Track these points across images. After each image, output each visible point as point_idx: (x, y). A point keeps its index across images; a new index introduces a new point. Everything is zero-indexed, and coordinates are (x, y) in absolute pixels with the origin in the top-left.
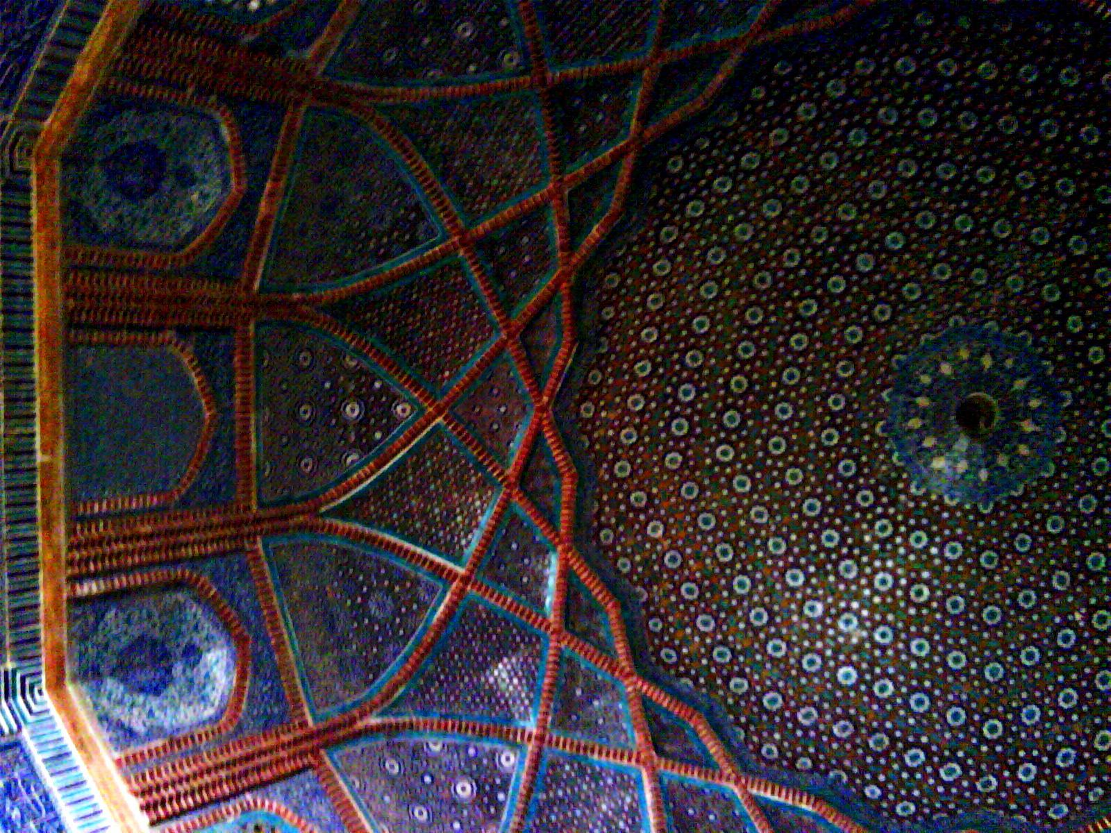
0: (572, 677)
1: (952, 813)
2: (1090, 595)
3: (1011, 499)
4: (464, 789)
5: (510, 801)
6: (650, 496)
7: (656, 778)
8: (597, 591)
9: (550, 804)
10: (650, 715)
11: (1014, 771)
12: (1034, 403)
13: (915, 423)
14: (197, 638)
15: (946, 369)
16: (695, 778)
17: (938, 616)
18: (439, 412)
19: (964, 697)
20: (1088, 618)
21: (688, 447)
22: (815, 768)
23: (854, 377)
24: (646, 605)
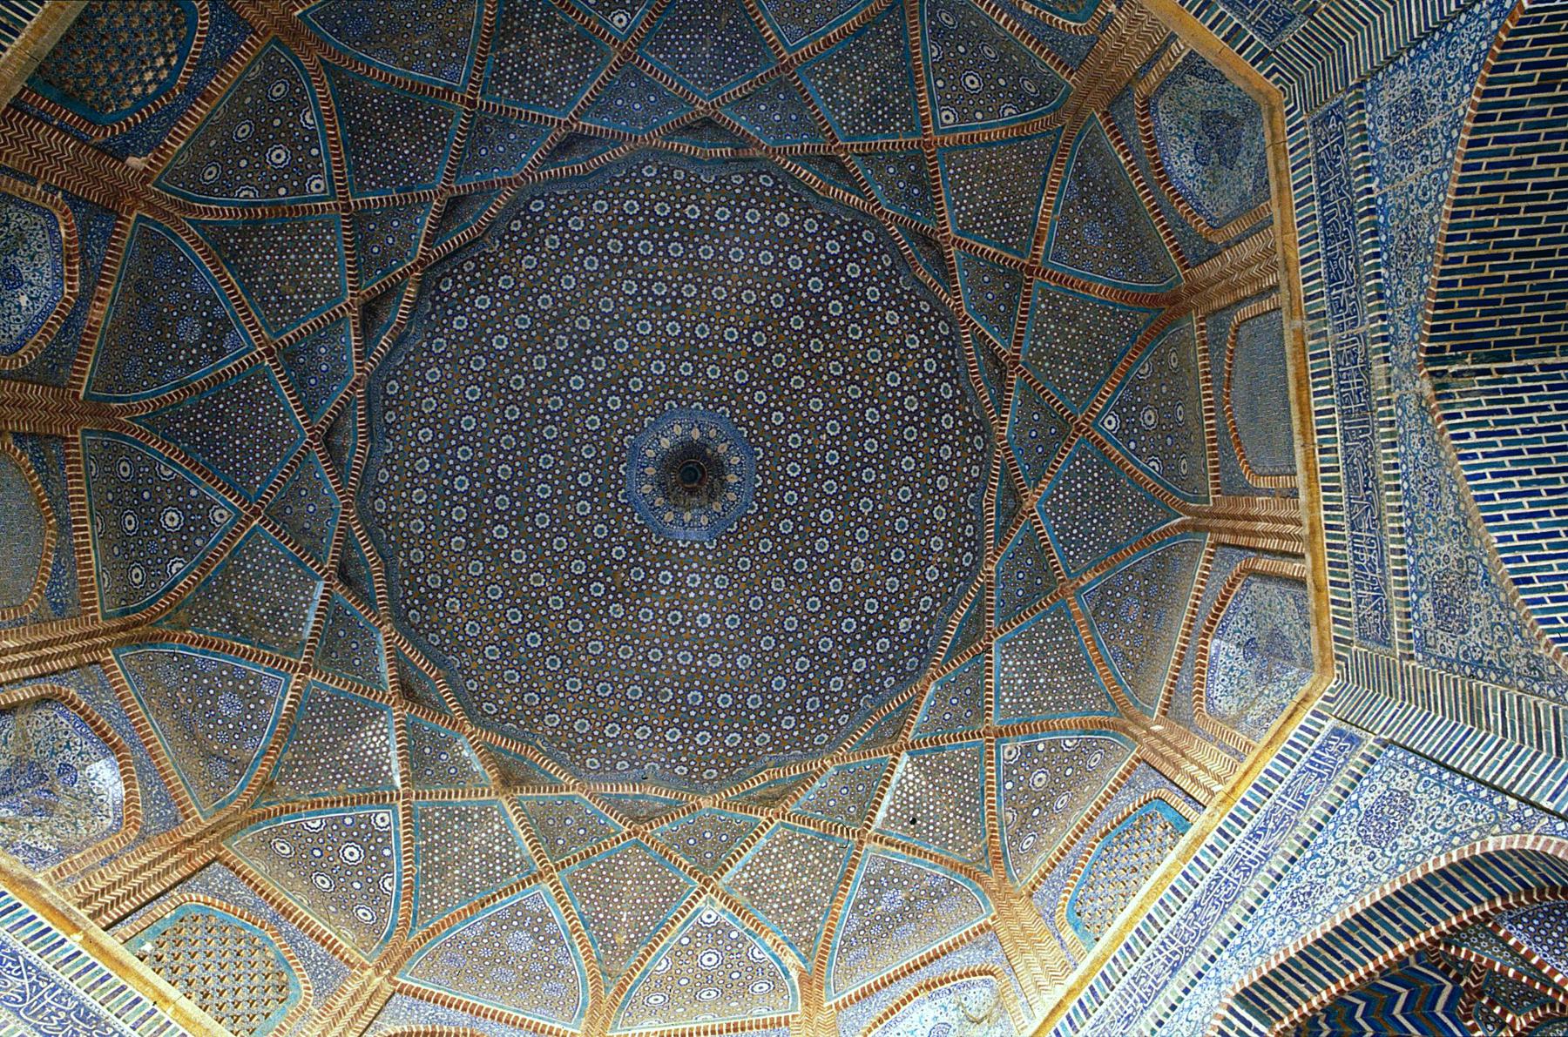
2: (801, 590)
6: (443, 576)
10: (490, 754)
11: (778, 725)
14: (69, 756)
18: (256, 513)
22: (632, 766)
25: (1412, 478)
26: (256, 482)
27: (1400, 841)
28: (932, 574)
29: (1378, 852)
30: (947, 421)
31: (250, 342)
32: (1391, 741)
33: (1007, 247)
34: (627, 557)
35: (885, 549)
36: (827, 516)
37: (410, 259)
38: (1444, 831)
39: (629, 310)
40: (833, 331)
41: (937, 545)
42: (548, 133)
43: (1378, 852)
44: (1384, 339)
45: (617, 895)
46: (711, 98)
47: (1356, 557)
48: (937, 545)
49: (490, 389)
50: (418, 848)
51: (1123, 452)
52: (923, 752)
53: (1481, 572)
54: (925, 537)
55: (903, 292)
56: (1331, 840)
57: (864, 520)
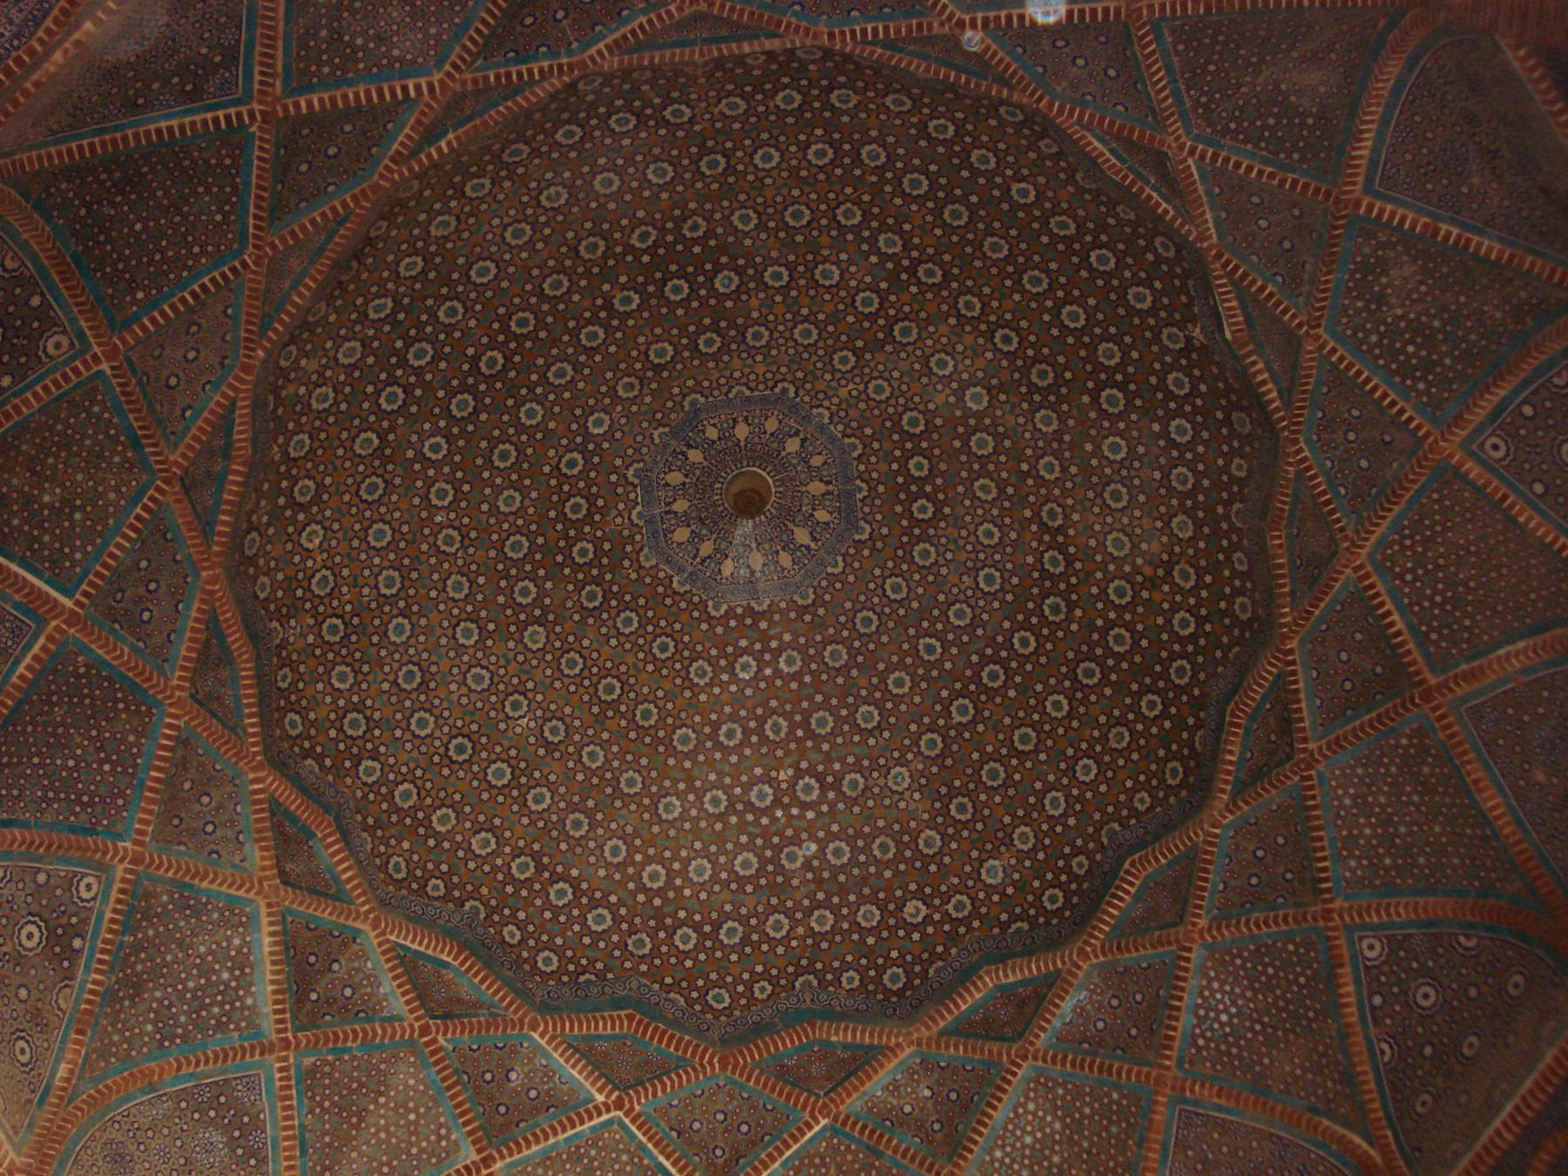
0: (183, 765)
1: (601, 976)
2: (803, 756)
3: (750, 611)
4: (31, 936)
5: (94, 949)
6: (321, 487)
7: (281, 917)
8: (236, 639)
9: (138, 947)
12: (822, 515)
13: (675, 478)
15: (742, 431)
16: (325, 914)
17: (623, 723)
19: (629, 829)
20: (792, 783)
21: (392, 429)
23: (633, 401)
24: (281, 647)
26: (135, 302)
28: (994, 872)
30: (1151, 705)
31: (248, 92)
33: (1423, 641)
34: (590, 564)
35: (950, 787)
36: (899, 683)
37: (570, 53)
39: (824, 240)
40: (1087, 471)
41: (1023, 839)
42: (920, 14)
45: (358, 1114)
46: (1197, 138)
48: (1023, 839)
49: (546, 240)
50: (121, 946)
51: (1359, 993)
52: (853, 1139)
54: (1014, 816)
55: (1226, 517)
57: (948, 727)
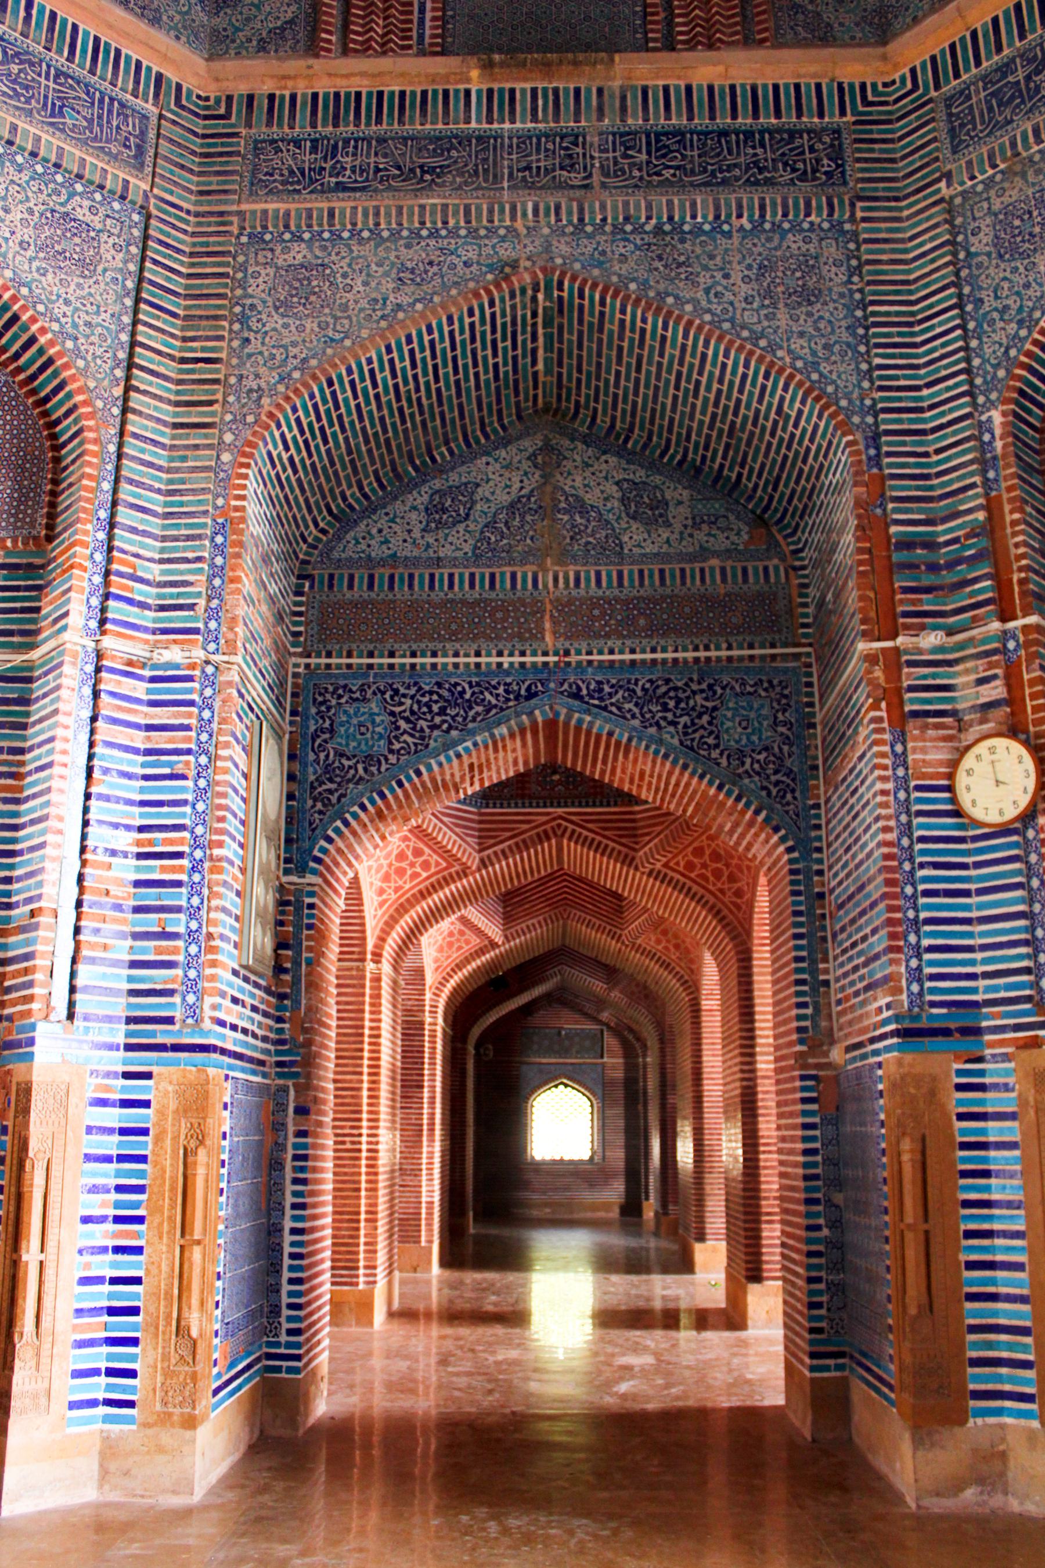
25: (432, 242)
27: (50, 276)
29: (30, 253)
32: (149, 216)
38: (75, 326)
43: (30, 253)
44: (581, 220)
47: (347, 142)
53: (338, 336)
56: (25, 177)
